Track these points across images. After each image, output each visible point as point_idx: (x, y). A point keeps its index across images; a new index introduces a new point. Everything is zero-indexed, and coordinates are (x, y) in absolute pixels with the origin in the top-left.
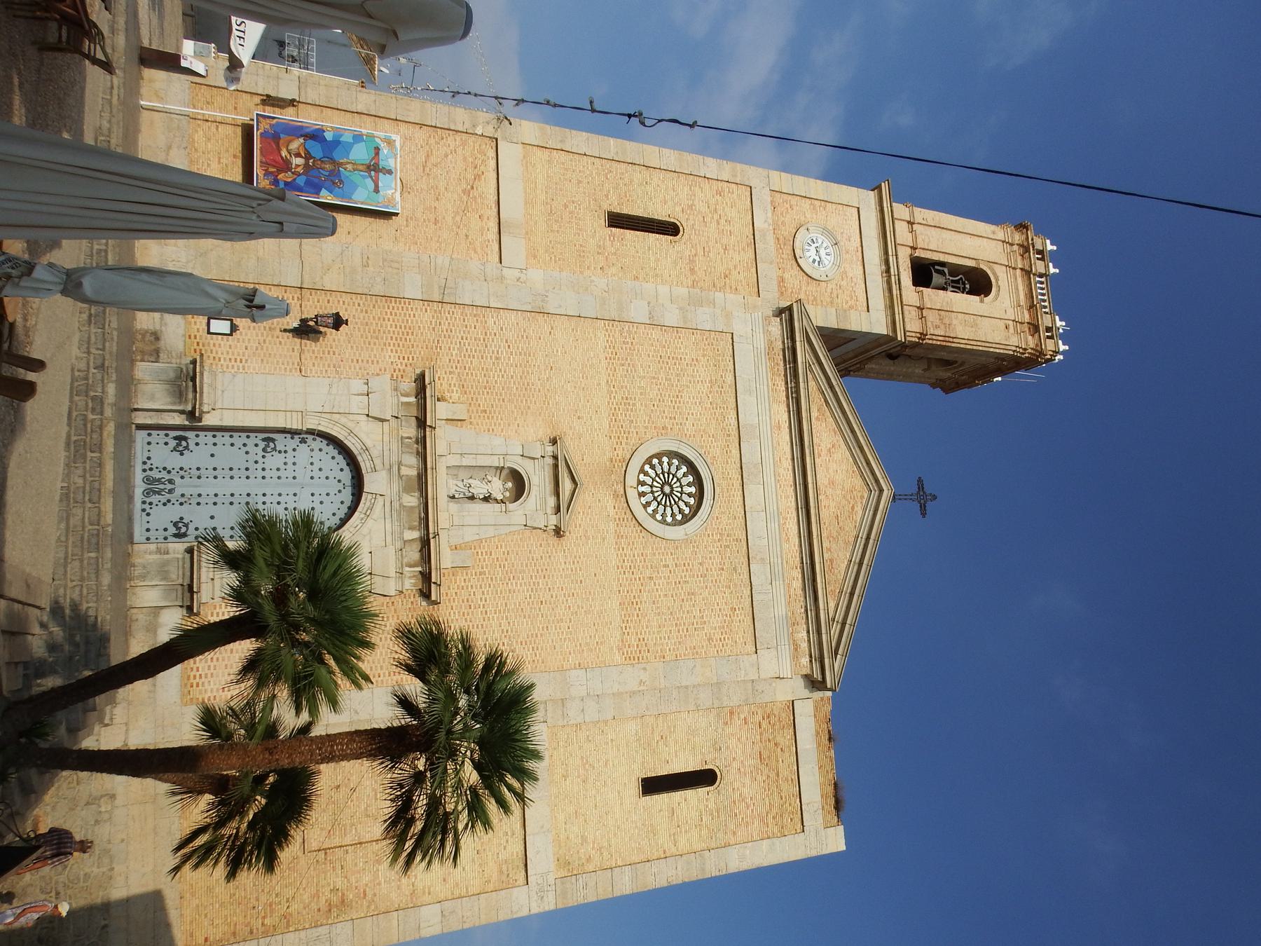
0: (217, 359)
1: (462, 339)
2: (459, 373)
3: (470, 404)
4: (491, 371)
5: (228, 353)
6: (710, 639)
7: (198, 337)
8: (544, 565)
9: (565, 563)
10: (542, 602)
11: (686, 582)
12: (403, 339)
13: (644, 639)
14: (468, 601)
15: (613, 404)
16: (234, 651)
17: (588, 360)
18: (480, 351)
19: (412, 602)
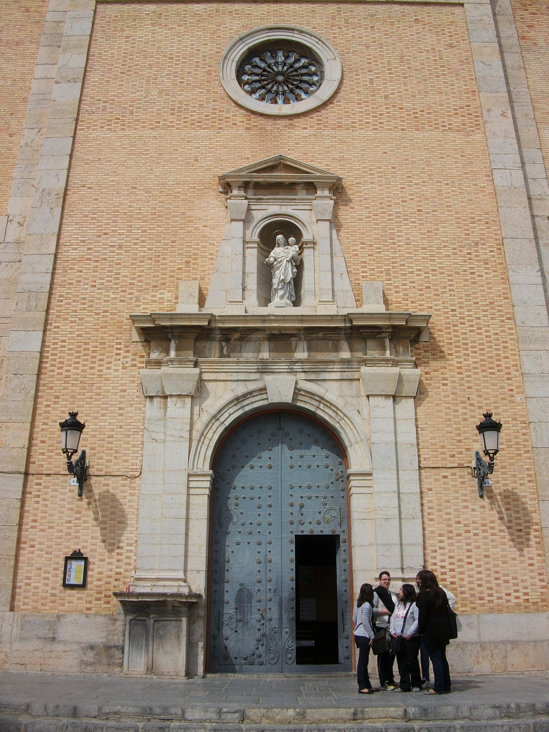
0: (118, 576)
1: (95, 286)
2: (138, 291)
3: (178, 279)
4: (136, 254)
5: (110, 563)
6: (451, 46)
7: (89, 599)
8: (375, 205)
9: (372, 183)
10: (419, 210)
11: (389, 63)
12: (94, 354)
13: (455, 110)
14: (421, 290)
15: (180, 124)
16: (487, 553)
17: (124, 148)
18: (110, 266)
19: (425, 351)
